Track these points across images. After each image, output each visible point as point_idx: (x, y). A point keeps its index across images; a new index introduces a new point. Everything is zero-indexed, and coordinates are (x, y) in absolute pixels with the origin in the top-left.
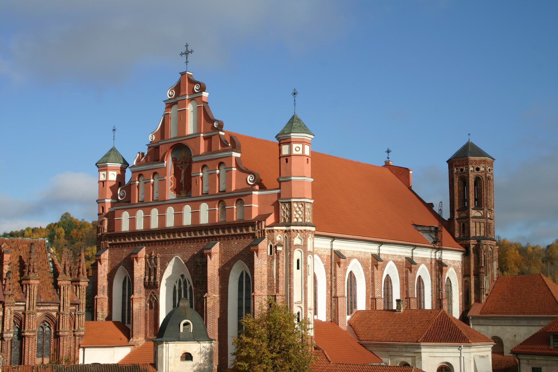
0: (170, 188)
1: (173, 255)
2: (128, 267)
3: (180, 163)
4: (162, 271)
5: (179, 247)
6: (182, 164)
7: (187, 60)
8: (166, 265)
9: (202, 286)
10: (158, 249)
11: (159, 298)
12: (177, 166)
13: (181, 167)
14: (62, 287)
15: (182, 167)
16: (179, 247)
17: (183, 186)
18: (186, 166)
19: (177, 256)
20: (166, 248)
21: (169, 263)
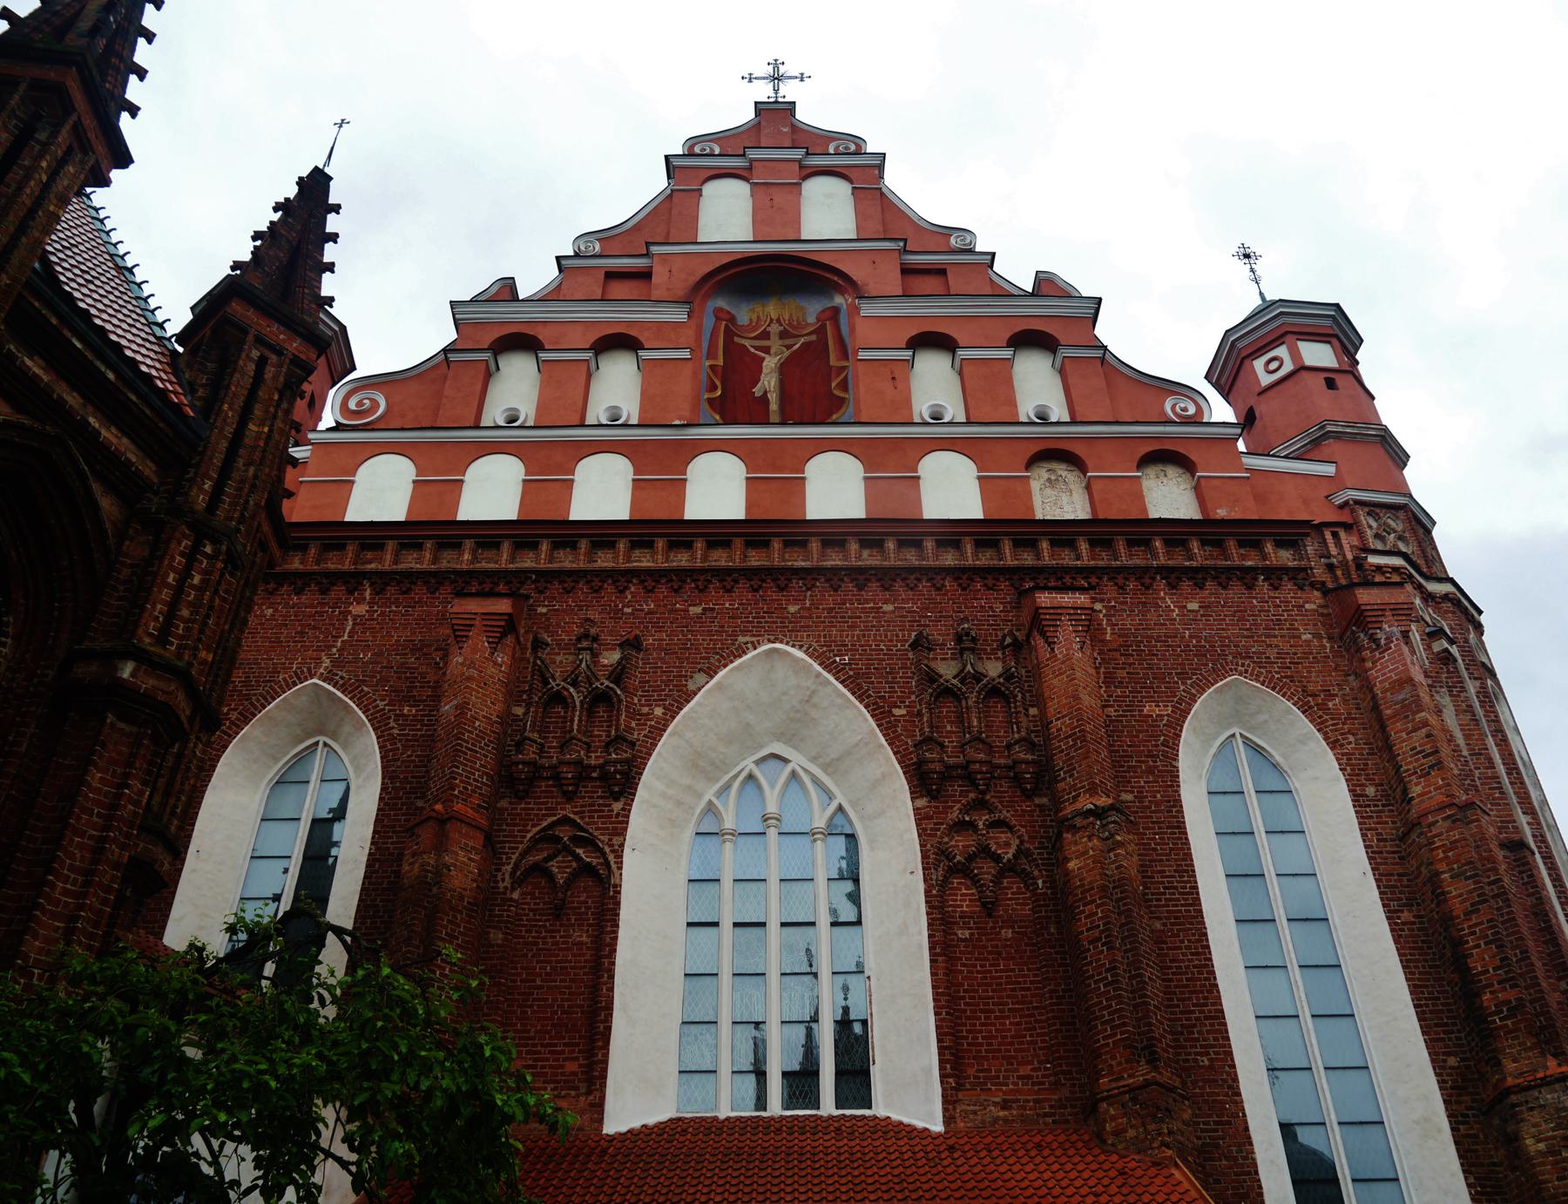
0: (706, 397)
1: (741, 639)
2: (365, 689)
3: (753, 335)
4: (659, 711)
5: (792, 609)
6: (769, 339)
7: (776, 93)
8: (691, 686)
9: (984, 793)
10: (628, 610)
11: (619, 856)
12: (736, 339)
13: (756, 348)
14: (255, 354)
15: (767, 350)
16: (792, 609)
17: (774, 406)
18: (789, 347)
19: (778, 645)
20: (696, 610)
21: (711, 673)
